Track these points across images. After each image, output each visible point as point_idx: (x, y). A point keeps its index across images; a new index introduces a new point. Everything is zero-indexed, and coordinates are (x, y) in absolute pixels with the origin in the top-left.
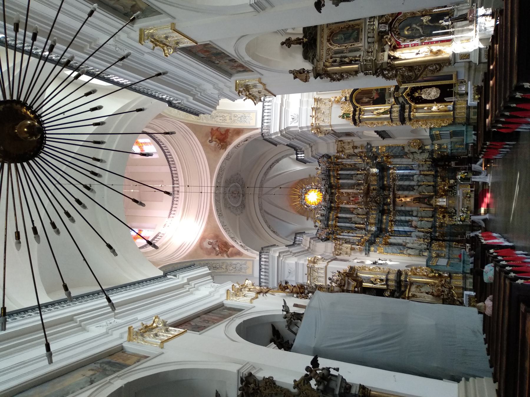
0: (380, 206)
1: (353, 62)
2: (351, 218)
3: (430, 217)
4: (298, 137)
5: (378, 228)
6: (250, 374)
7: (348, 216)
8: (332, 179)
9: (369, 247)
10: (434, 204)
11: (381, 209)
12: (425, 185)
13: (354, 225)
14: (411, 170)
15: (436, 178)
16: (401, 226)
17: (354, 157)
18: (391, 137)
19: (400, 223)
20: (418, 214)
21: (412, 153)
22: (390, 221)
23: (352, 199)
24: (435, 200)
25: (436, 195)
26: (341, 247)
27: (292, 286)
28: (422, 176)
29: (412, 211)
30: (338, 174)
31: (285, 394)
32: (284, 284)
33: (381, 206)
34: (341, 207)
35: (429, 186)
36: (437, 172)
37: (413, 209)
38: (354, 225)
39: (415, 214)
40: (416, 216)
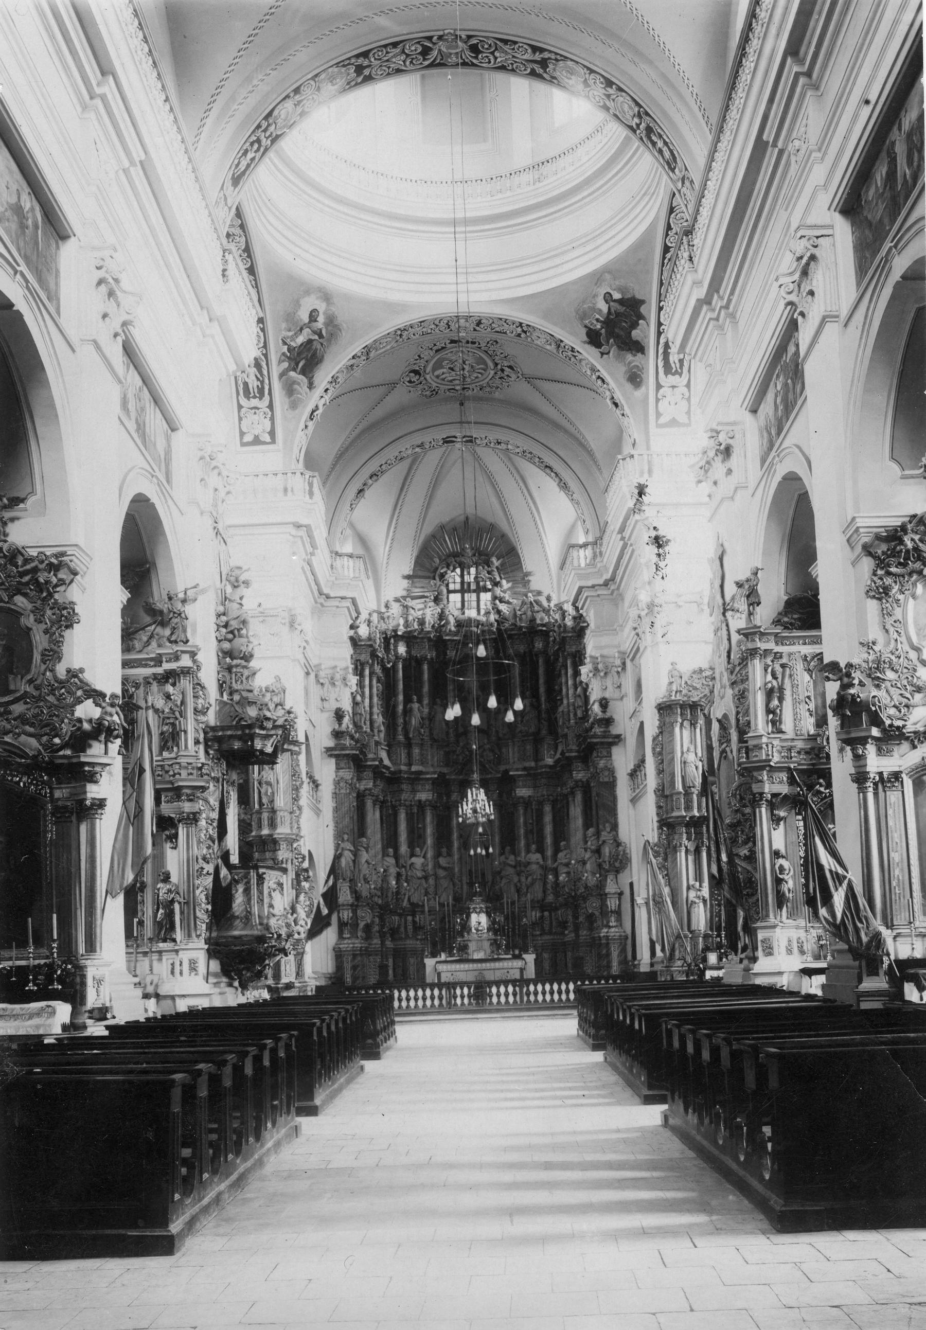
1: (771, 716)
4: (629, 550)
6: (75, 574)
27: (241, 598)
31: (52, 650)
32: (242, 578)
39: (443, 861)
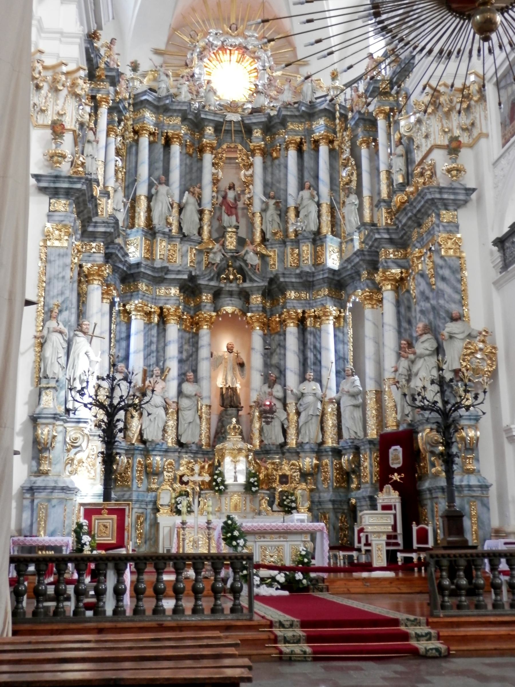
0: (211, 280)
2: (167, 183)
3: (178, 435)
5: (138, 265)
7: (175, 175)
8: (300, 127)
9: (68, 193)
10: (228, 445)
11: (202, 282)
12: (287, 419)
13: (142, 190)
14: (338, 373)
15: (313, 451)
16: (148, 345)
17: (399, 163)
18: (505, 266)
19: (155, 339)
20: (188, 397)
21: (439, 350)
22: (161, 308)
23: (231, 195)
24: (240, 450)
25: (256, 454)
26: (65, 92)
28: (319, 406)
29: (196, 380)
30: (316, 143)
33: (212, 283)
34: (201, 160)
35: (285, 432)
36: (337, 453)
37: (205, 384)
38: (142, 190)
39: (188, 388)
40: (180, 393)
